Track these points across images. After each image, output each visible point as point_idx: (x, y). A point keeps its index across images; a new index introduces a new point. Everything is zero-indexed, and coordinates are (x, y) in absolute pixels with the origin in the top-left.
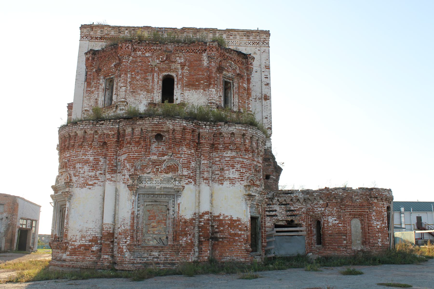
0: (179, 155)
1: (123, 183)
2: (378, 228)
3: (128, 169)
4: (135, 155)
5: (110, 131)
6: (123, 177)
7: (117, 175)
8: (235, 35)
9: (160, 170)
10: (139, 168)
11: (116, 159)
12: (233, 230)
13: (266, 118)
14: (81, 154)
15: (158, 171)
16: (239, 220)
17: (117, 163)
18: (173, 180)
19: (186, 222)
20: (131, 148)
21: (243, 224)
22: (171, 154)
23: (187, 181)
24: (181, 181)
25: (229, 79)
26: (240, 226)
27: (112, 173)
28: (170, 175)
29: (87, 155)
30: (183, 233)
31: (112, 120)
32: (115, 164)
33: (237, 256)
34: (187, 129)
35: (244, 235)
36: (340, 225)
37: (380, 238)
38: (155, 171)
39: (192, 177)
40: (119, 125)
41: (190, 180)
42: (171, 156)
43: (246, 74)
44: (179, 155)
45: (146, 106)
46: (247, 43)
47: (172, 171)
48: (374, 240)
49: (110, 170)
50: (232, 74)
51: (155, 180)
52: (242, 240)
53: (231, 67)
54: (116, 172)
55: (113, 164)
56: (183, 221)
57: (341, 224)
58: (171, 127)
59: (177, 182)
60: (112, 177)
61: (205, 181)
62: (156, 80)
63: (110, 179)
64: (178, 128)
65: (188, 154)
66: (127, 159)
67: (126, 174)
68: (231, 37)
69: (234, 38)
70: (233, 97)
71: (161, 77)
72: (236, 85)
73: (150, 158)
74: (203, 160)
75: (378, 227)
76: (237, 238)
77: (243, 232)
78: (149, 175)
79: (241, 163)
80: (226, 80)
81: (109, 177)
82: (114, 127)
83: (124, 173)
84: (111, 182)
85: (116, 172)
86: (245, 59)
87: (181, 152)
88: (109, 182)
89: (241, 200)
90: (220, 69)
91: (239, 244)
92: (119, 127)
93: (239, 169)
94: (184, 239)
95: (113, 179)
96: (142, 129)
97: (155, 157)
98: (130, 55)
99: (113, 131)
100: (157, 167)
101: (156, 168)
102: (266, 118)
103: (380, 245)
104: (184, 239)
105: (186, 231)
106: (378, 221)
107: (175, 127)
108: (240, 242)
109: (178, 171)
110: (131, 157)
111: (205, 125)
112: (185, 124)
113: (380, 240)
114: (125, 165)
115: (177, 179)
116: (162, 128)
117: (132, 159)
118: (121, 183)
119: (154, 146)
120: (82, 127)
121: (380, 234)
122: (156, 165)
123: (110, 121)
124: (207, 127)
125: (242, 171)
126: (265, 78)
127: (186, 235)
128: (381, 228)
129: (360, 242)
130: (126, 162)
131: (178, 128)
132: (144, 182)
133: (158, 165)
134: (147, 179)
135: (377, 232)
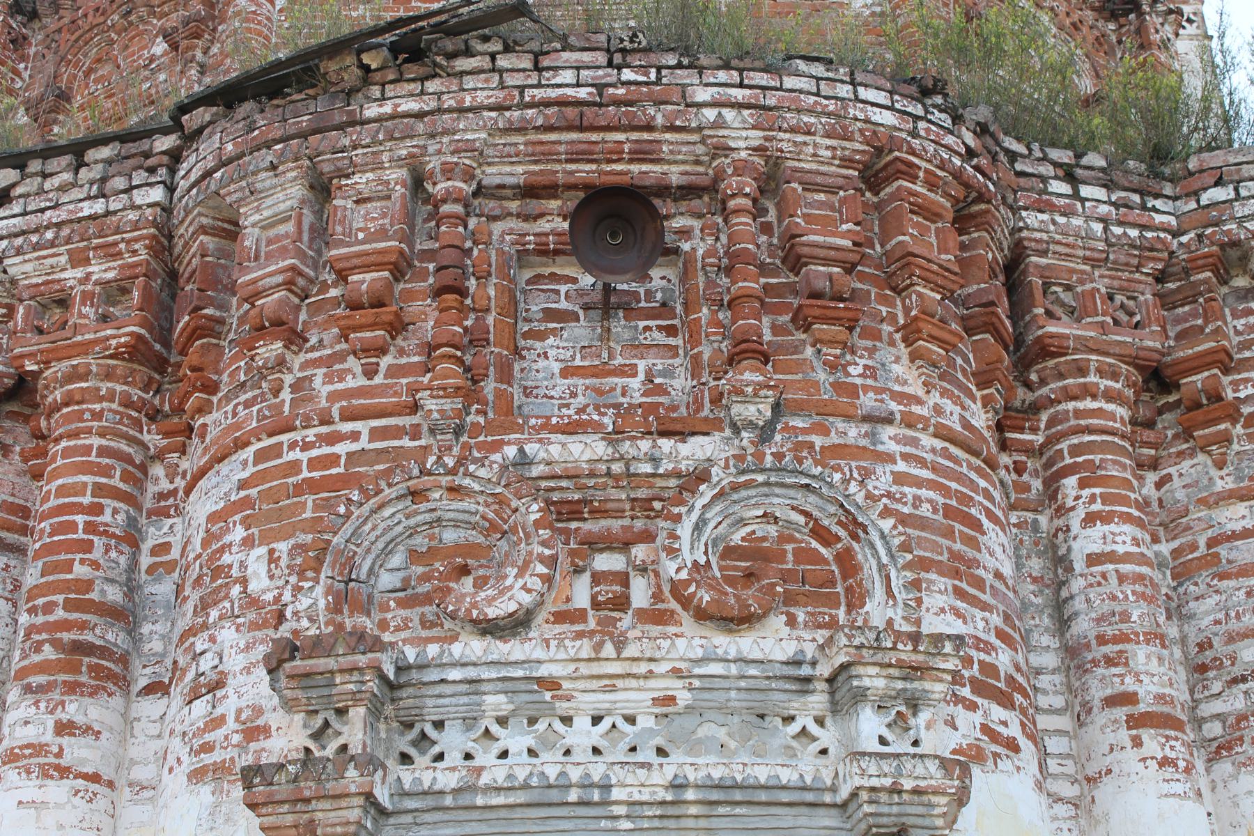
0: (854, 433)
1: (197, 776)
3: (253, 602)
4: (342, 449)
5: (78, 259)
6: (200, 707)
7: (129, 721)
9: (640, 594)
10: (387, 580)
11: (132, 539)
15: (621, 603)
17: (131, 588)
18: (818, 700)
22: (757, 411)
23: (969, 724)
24: (914, 705)
27: (72, 688)
28: (774, 641)
31: (105, 152)
32: (114, 595)
38: (582, 598)
40: (171, 189)
41: (998, 712)
42: (765, 433)
44: (854, 433)
47: (790, 599)
49: (48, 652)
51: (591, 701)
54: (123, 682)
55: (88, 585)
58: (742, 135)
59: (869, 725)
60: (63, 728)
61: (1152, 742)
63: (39, 749)
64: (815, 153)
65: (943, 433)
66: (246, 503)
67: (234, 662)
73: (524, 461)
74: (1090, 519)
78: (513, 649)
81: (28, 734)
83: (206, 664)
84: (57, 790)
85: (123, 682)
86: (1113, 16)
87: (867, 401)
88: (30, 789)
92: (167, 210)
95: (78, 752)
96: (418, 182)
97: (584, 450)
99: (109, 252)
100: (606, 562)
101: (597, 578)
107: (785, 141)
109: (856, 599)
110: (294, 466)
111: (1069, 176)
112: (887, 118)
114: (217, 572)
115: (873, 680)
116: (642, 154)
117: (312, 486)
118: (175, 782)
119: (549, 362)
122: (595, 544)
123: (80, 164)
124: (1085, 191)
130: (238, 533)
131: (815, 153)
132: (453, 740)
133: (625, 546)
134: (495, 702)
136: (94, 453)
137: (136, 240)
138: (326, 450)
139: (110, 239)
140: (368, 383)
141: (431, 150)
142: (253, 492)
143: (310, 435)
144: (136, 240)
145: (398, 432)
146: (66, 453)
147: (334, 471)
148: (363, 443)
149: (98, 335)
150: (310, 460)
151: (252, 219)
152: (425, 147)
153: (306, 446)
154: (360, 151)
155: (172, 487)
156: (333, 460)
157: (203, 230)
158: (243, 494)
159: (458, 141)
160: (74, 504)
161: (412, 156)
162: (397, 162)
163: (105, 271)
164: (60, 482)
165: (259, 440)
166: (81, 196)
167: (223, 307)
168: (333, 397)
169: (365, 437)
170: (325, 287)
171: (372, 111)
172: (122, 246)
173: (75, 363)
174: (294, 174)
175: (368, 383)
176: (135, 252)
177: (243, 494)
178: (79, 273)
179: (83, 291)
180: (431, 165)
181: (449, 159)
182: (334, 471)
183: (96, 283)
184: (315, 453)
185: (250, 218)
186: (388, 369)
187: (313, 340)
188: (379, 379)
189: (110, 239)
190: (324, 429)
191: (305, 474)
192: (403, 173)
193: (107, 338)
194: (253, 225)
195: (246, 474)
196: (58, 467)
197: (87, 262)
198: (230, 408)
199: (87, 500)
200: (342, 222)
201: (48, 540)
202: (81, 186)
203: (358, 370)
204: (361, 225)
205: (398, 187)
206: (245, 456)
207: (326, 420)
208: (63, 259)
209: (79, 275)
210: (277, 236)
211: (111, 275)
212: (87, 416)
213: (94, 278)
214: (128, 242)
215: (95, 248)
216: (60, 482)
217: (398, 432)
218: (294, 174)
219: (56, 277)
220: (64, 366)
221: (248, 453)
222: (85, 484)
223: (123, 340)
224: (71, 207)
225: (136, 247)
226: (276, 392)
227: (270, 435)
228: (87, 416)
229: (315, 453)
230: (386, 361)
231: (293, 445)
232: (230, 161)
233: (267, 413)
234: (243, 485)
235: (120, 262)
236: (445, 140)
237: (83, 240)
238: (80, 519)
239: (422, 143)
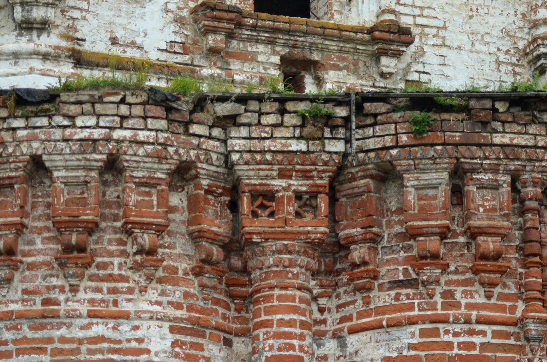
4: (477, 340)
5: (282, 175)
14: (84, 309)
20: (448, 295)
29: (126, 316)
45: (179, 20)
82: (315, 146)
99: (305, 175)
110: (449, 345)
120: (97, 134)
123: (282, 112)
136: (297, 300)
137: (324, 171)
138: (467, 339)
139: (308, 167)
140: (488, 302)
141: (528, 168)
142: (423, 354)
143: (457, 328)
144: (324, 171)
145: (507, 335)
146: (280, 298)
147: (473, 353)
148: (489, 339)
149: (301, 229)
150: (459, 344)
151: (412, 183)
152: (525, 166)
153: (456, 335)
154: (488, 162)
155: (322, 318)
156: (470, 346)
157: (371, 177)
158: (413, 353)
159: (543, 166)
160: (291, 333)
161: (516, 170)
162: (506, 172)
163: (301, 185)
164: (280, 316)
165: (424, 323)
166: (288, 135)
167: (380, 226)
168: (470, 306)
169: (489, 335)
170: (455, 235)
171: (498, 139)
172: (315, 173)
173: (286, 242)
174: (446, 166)
175: (488, 302)
176: (321, 178)
177: (413, 353)
178: (283, 183)
179: (287, 196)
180: (526, 177)
181: (536, 175)
182: (473, 353)
183: (294, 191)
184: (461, 339)
185: (411, 181)
186: (498, 295)
187: (452, 268)
188: (493, 301)
189: (308, 167)
190: (466, 327)
191: (456, 351)
192: (508, 178)
193: (309, 232)
194: (412, 186)
195: (415, 341)
196: (273, 306)
197: (290, 177)
198: (393, 293)
199: (297, 331)
200: (473, 201)
201: (277, 353)
202: (287, 127)
203: (483, 293)
204: (481, 203)
205: (505, 185)
206: (413, 330)
207: (467, 321)
208: (275, 173)
209: (284, 185)
210: (426, 195)
211: (304, 189)
212: (290, 275)
213: (293, 188)
214: (319, 172)
215: (297, 171)
216: (280, 316)
217: (507, 335)
218: (446, 166)
219: (268, 182)
220: (280, 244)
221: (416, 329)
222: (295, 320)
223: (319, 235)
224: (283, 141)
225: (323, 175)
226: (431, 296)
227: (432, 322)
228: (290, 275)
229: (461, 339)
230: (498, 290)
231: (447, 332)
232: (403, 147)
233: (425, 306)
234: (411, 347)
235: (311, 182)
236: (537, 164)
237: (290, 165)
238: (296, 342)
239: (523, 163)
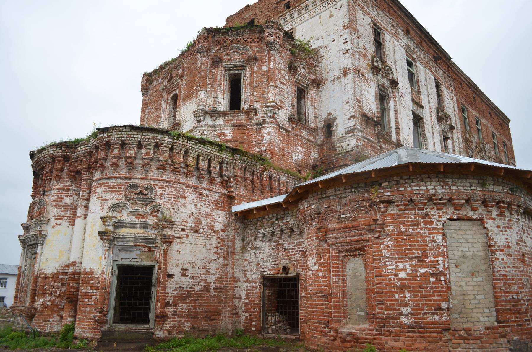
2: (400, 279)
8: (307, 6)
12: (85, 289)
13: (347, 103)
16: (92, 273)
19: (45, 278)
21: (97, 279)
25: (238, 70)
26: (92, 282)
30: (40, 292)
33: (84, 328)
34: (56, 157)
35: (96, 295)
36: (320, 274)
37: (406, 305)
39: (63, 216)
43: (267, 53)
46: (322, 7)
48: (386, 309)
50: (239, 61)
52: (93, 303)
53: (237, 52)
56: (42, 276)
57: (321, 271)
62: (163, 106)
65: (58, 189)
68: (303, 11)
69: (306, 10)
70: (245, 91)
71: (169, 100)
72: (248, 73)
75: (402, 275)
76: (86, 300)
77: (95, 291)
79: (105, 186)
80: (231, 72)
89: (97, 241)
90: (216, 62)
91: (88, 309)
93: (100, 196)
94: (41, 300)
98: (148, 89)
102: (347, 103)
103: (407, 323)
104: (41, 300)
105: (45, 290)
106: (401, 260)
108: (90, 306)
112: (52, 152)
113: (406, 310)
121: (408, 295)
125: (104, 198)
126: (344, 43)
127: (44, 295)
128: (412, 277)
129: (362, 313)
135: (398, 288)
